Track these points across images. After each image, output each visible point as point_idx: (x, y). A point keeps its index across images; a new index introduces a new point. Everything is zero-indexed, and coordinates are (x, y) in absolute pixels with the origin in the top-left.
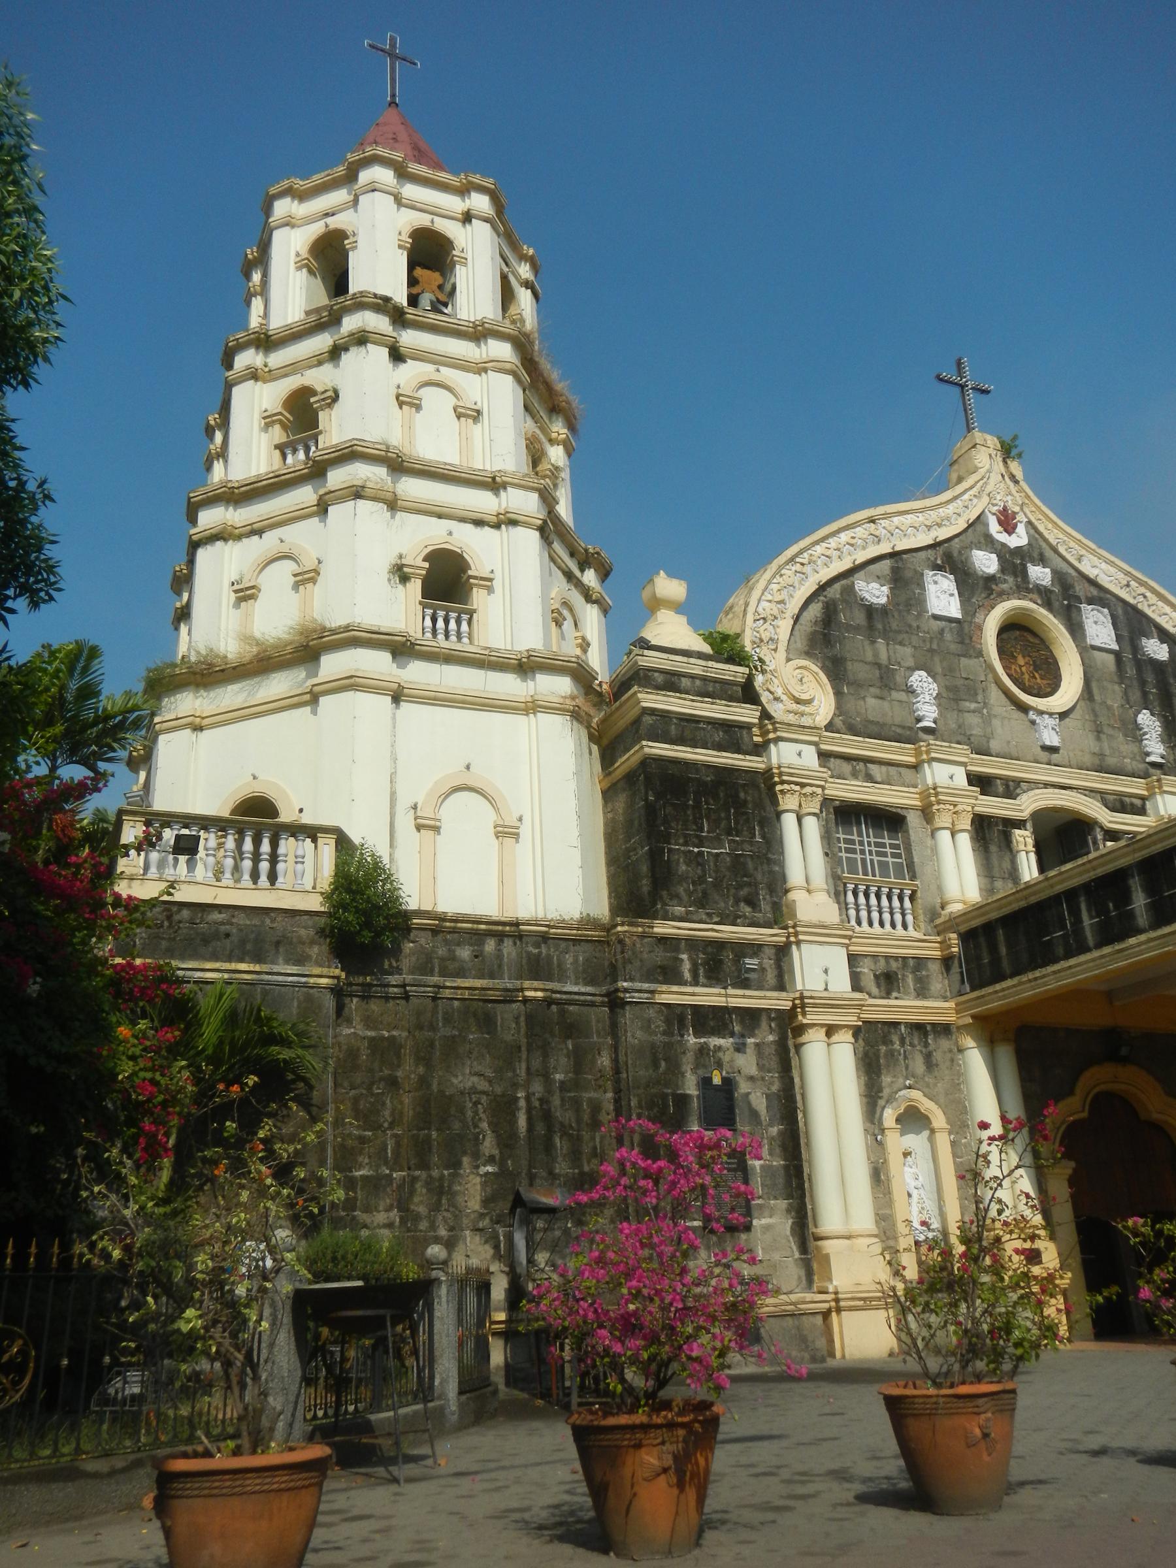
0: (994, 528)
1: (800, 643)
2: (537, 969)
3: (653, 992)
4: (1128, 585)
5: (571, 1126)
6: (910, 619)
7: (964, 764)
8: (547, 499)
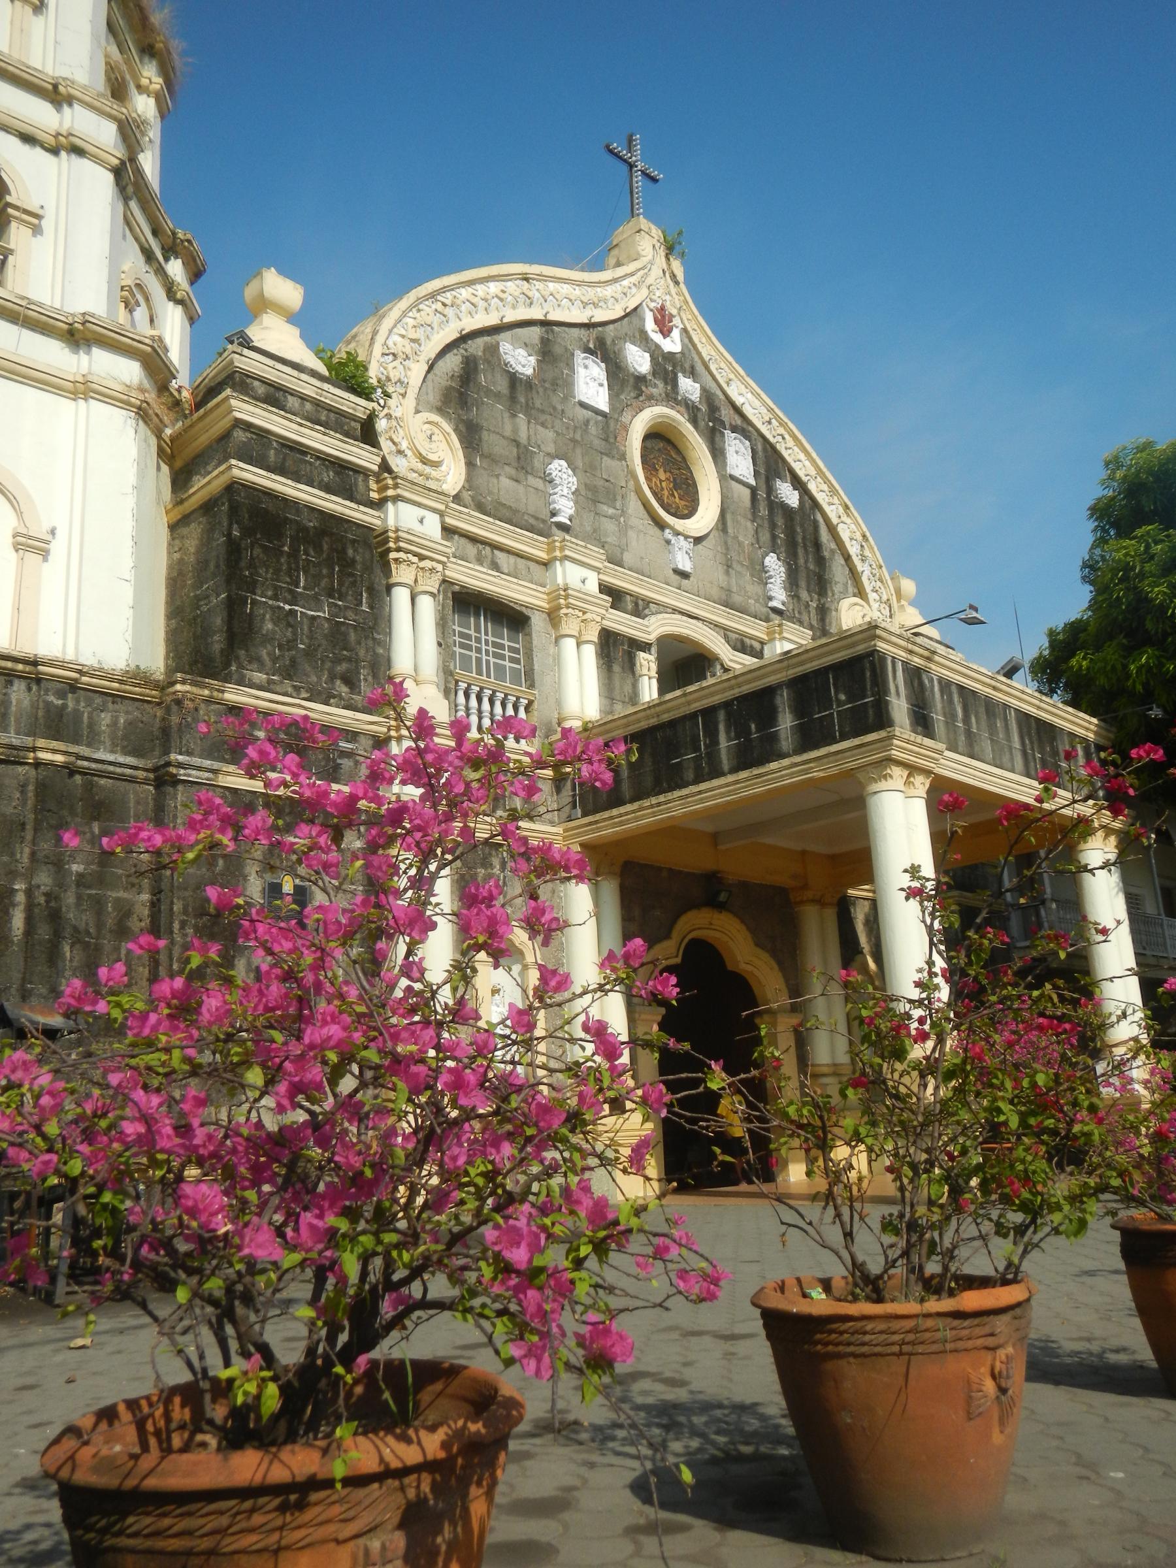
0: (650, 325)
1: (433, 397)
2: (57, 725)
3: (215, 772)
4: (769, 422)
5: (88, 933)
6: (555, 400)
7: (597, 570)
8: (129, 132)
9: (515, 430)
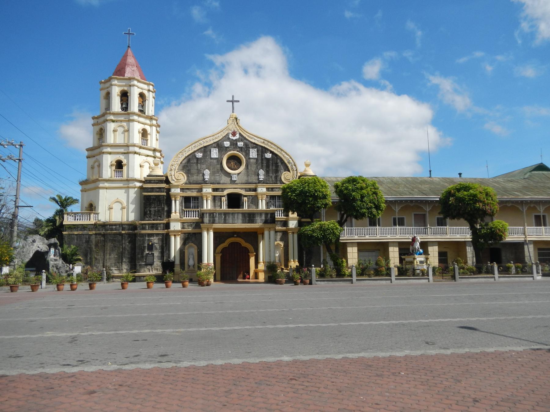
9: (198, 167)
